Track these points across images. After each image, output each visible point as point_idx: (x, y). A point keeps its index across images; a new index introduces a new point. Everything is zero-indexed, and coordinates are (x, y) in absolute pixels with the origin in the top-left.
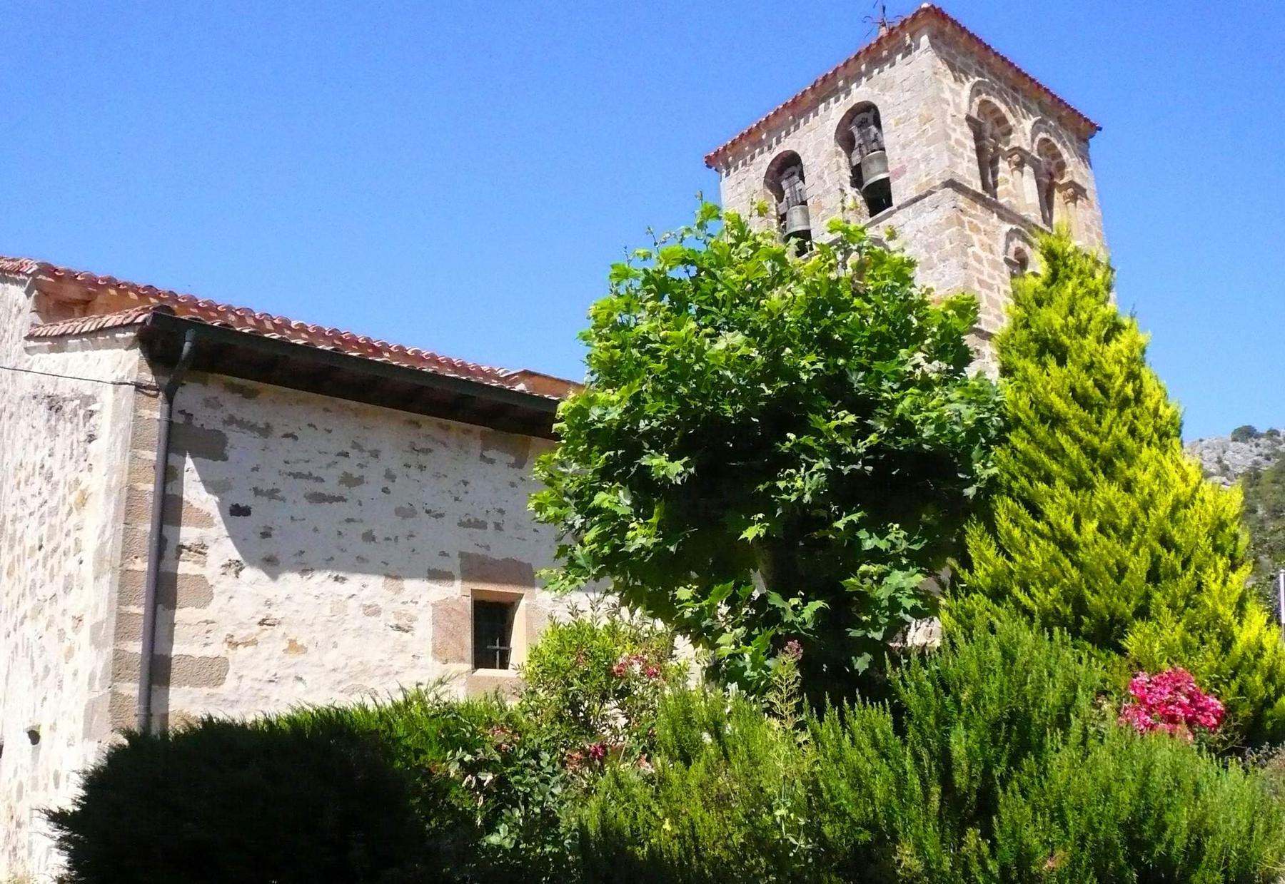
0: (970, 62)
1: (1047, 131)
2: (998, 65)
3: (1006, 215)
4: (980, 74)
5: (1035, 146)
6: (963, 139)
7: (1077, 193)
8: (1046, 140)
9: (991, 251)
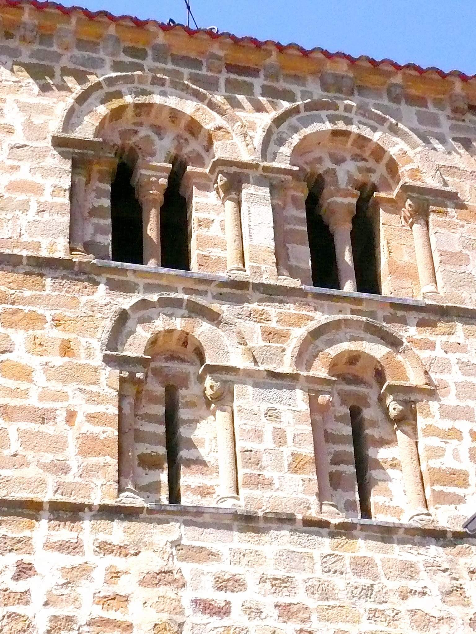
0: (102, 54)
1: (333, 119)
2: (181, 45)
3: (141, 282)
4: (117, 66)
5: (286, 150)
6: (37, 179)
7: (426, 203)
8: (335, 133)
9: (66, 349)
